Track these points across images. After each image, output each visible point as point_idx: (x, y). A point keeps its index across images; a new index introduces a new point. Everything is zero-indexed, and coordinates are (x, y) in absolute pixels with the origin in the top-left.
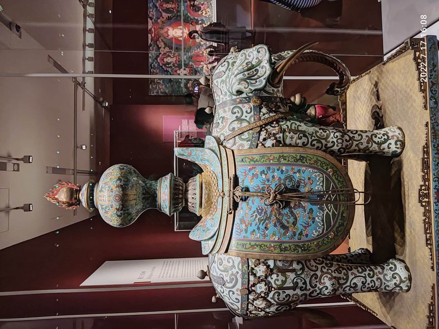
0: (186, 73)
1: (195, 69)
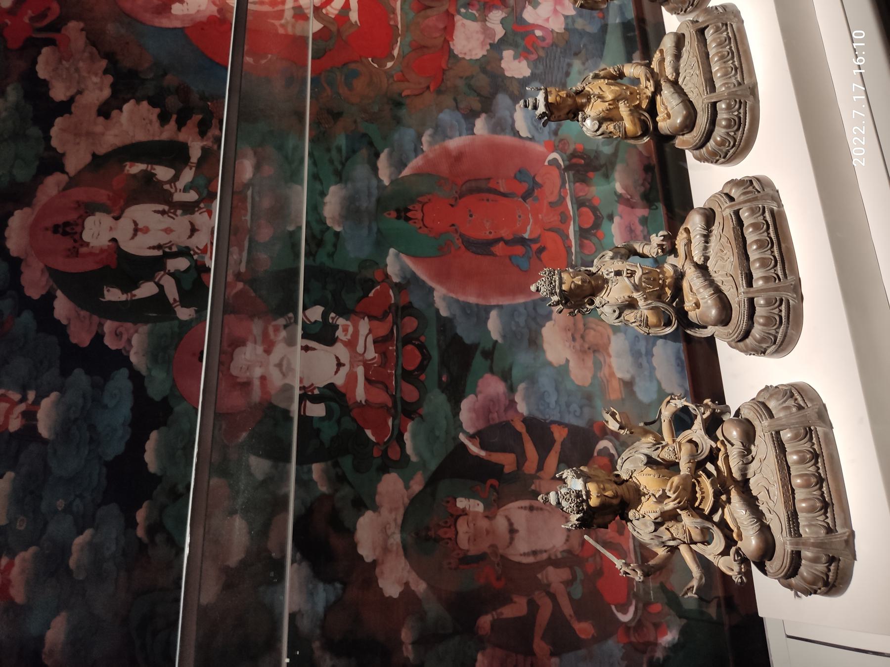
0: (339, 380)
1: (445, 325)
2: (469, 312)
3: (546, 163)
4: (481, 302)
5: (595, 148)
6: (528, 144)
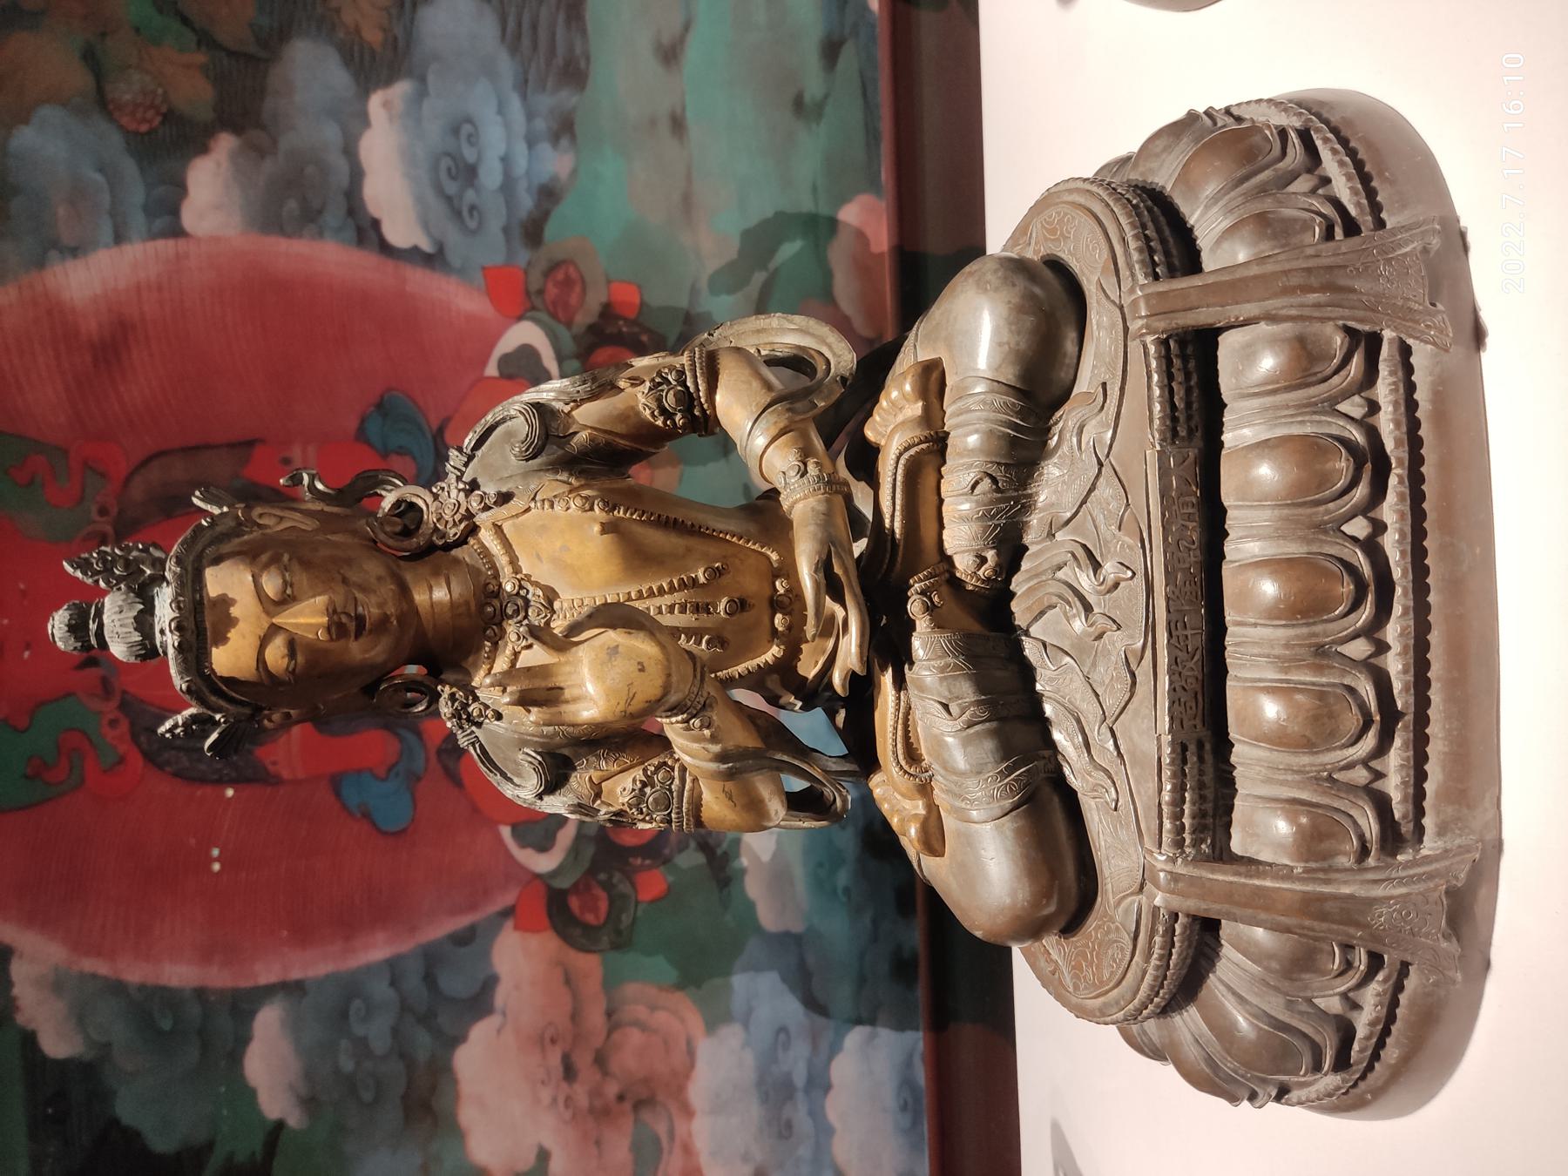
2: (166, 1024)
3: (492, 370)
4: (218, 977)
5: (683, 302)
6: (419, 280)
